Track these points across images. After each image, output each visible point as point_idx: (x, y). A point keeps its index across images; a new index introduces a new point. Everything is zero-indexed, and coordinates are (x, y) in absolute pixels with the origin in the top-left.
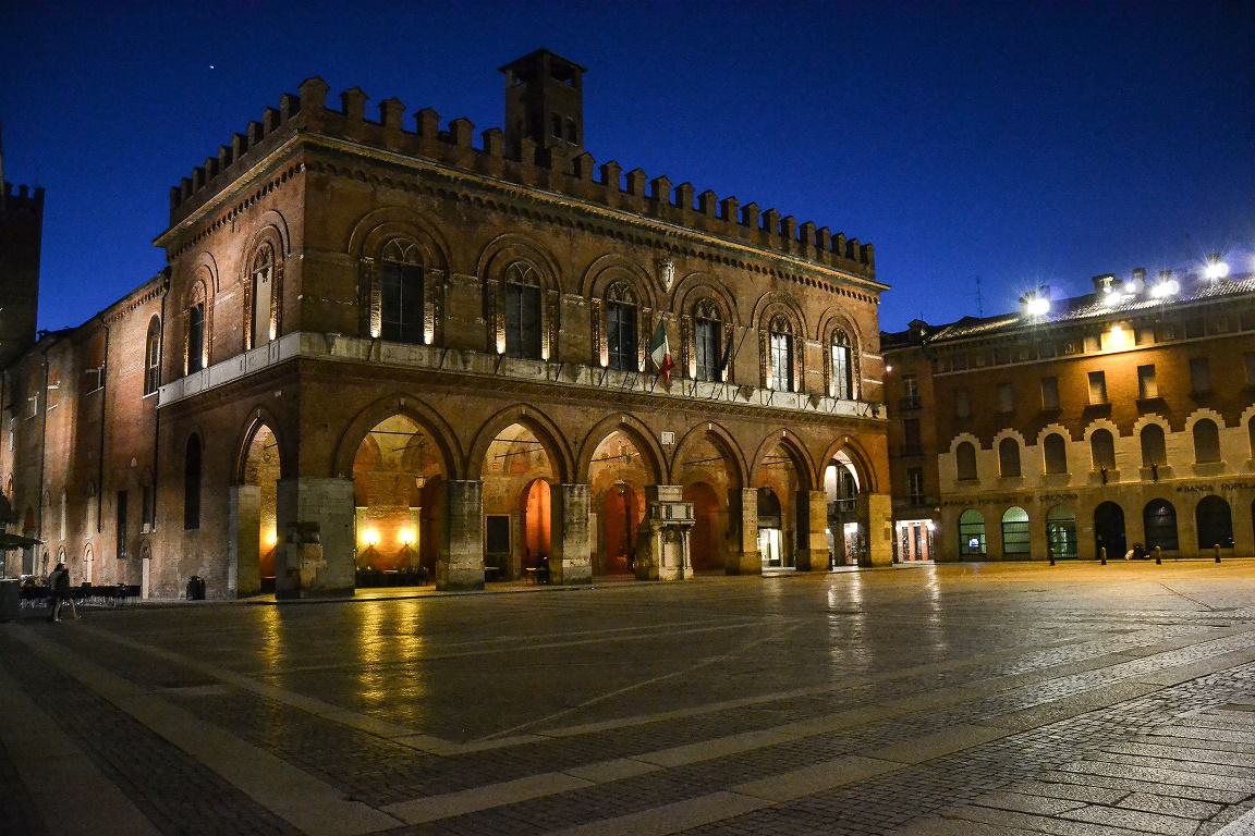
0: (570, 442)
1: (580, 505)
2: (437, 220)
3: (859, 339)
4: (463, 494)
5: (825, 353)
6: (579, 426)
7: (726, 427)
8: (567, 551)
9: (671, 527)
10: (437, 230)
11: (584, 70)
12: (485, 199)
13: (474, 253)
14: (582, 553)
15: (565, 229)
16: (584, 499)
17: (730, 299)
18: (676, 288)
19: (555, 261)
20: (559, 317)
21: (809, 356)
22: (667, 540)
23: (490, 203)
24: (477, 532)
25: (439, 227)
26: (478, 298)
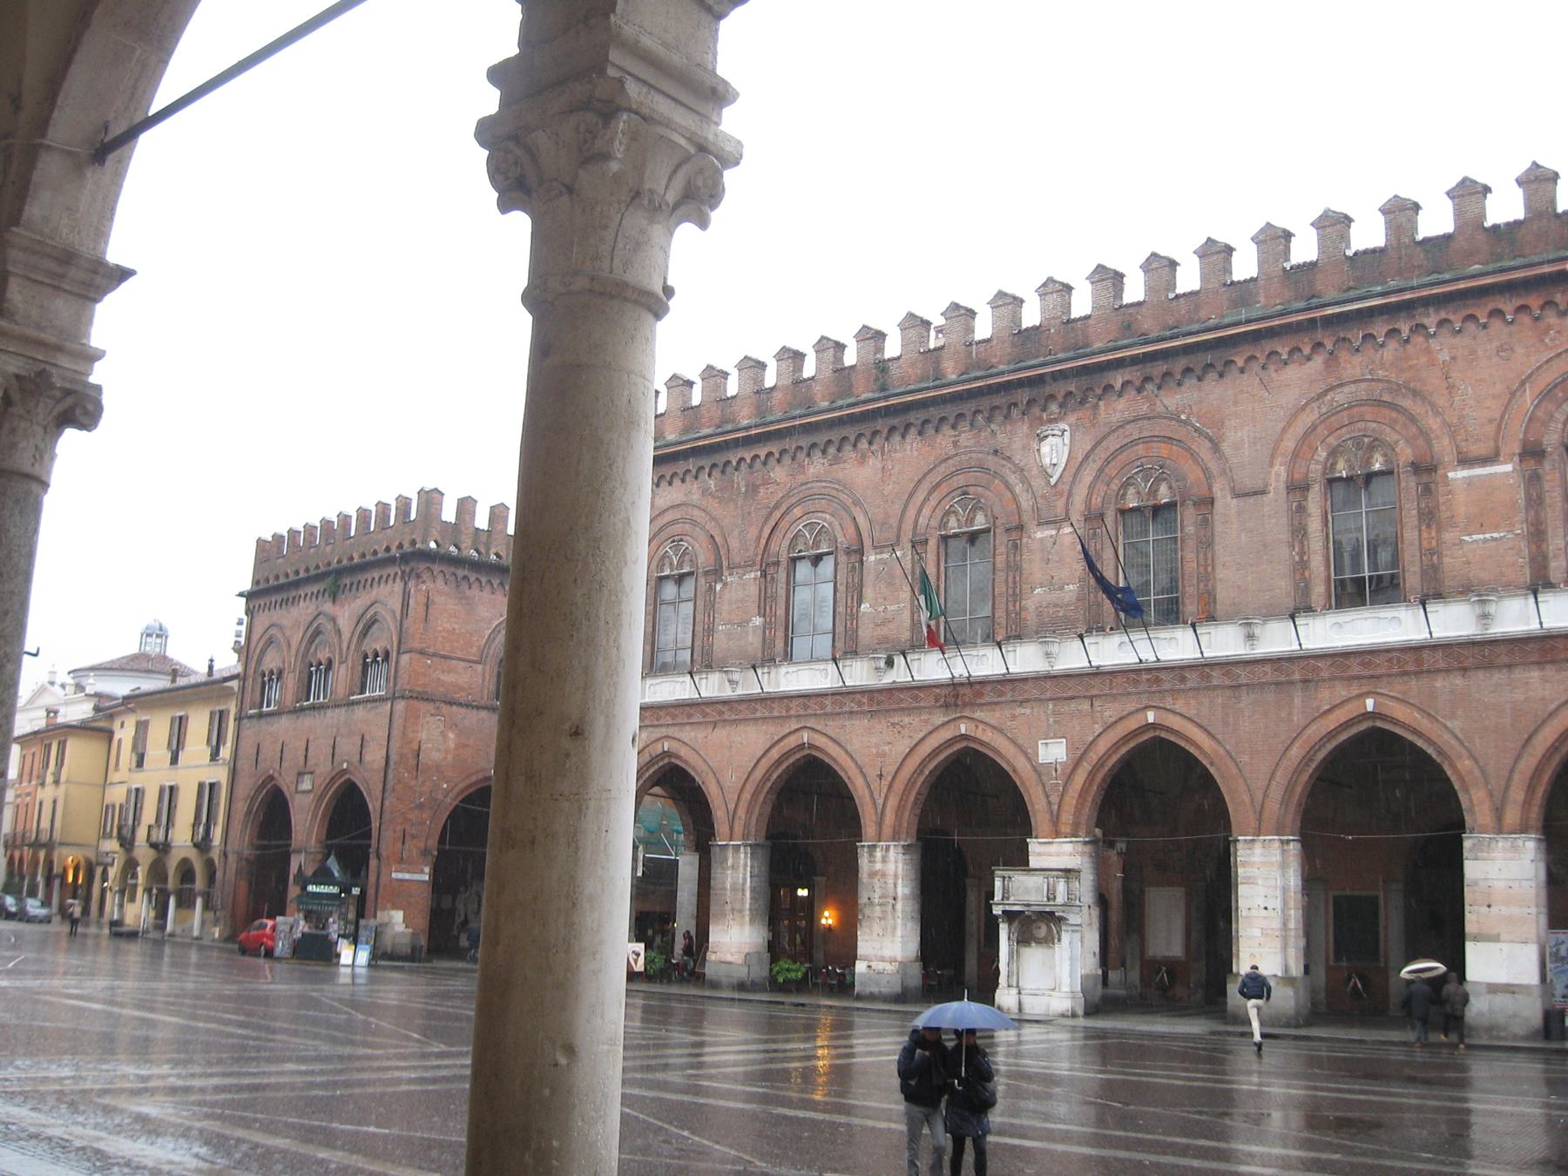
0: (872, 773)
1: (884, 875)
2: (713, 505)
4: (726, 860)
6: (886, 748)
7: (1192, 713)
8: (863, 947)
10: (713, 519)
12: (762, 453)
13: (753, 532)
14: (887, 953)
15: (874, 447)
16: (891, 867)
17: (1203, 449)
18: (1075, 467)
19: (857, 503)
21: (1461, 505)
23: (770, 454)
24: (741, 911)
25: (714, 513)
26: (753, 590)
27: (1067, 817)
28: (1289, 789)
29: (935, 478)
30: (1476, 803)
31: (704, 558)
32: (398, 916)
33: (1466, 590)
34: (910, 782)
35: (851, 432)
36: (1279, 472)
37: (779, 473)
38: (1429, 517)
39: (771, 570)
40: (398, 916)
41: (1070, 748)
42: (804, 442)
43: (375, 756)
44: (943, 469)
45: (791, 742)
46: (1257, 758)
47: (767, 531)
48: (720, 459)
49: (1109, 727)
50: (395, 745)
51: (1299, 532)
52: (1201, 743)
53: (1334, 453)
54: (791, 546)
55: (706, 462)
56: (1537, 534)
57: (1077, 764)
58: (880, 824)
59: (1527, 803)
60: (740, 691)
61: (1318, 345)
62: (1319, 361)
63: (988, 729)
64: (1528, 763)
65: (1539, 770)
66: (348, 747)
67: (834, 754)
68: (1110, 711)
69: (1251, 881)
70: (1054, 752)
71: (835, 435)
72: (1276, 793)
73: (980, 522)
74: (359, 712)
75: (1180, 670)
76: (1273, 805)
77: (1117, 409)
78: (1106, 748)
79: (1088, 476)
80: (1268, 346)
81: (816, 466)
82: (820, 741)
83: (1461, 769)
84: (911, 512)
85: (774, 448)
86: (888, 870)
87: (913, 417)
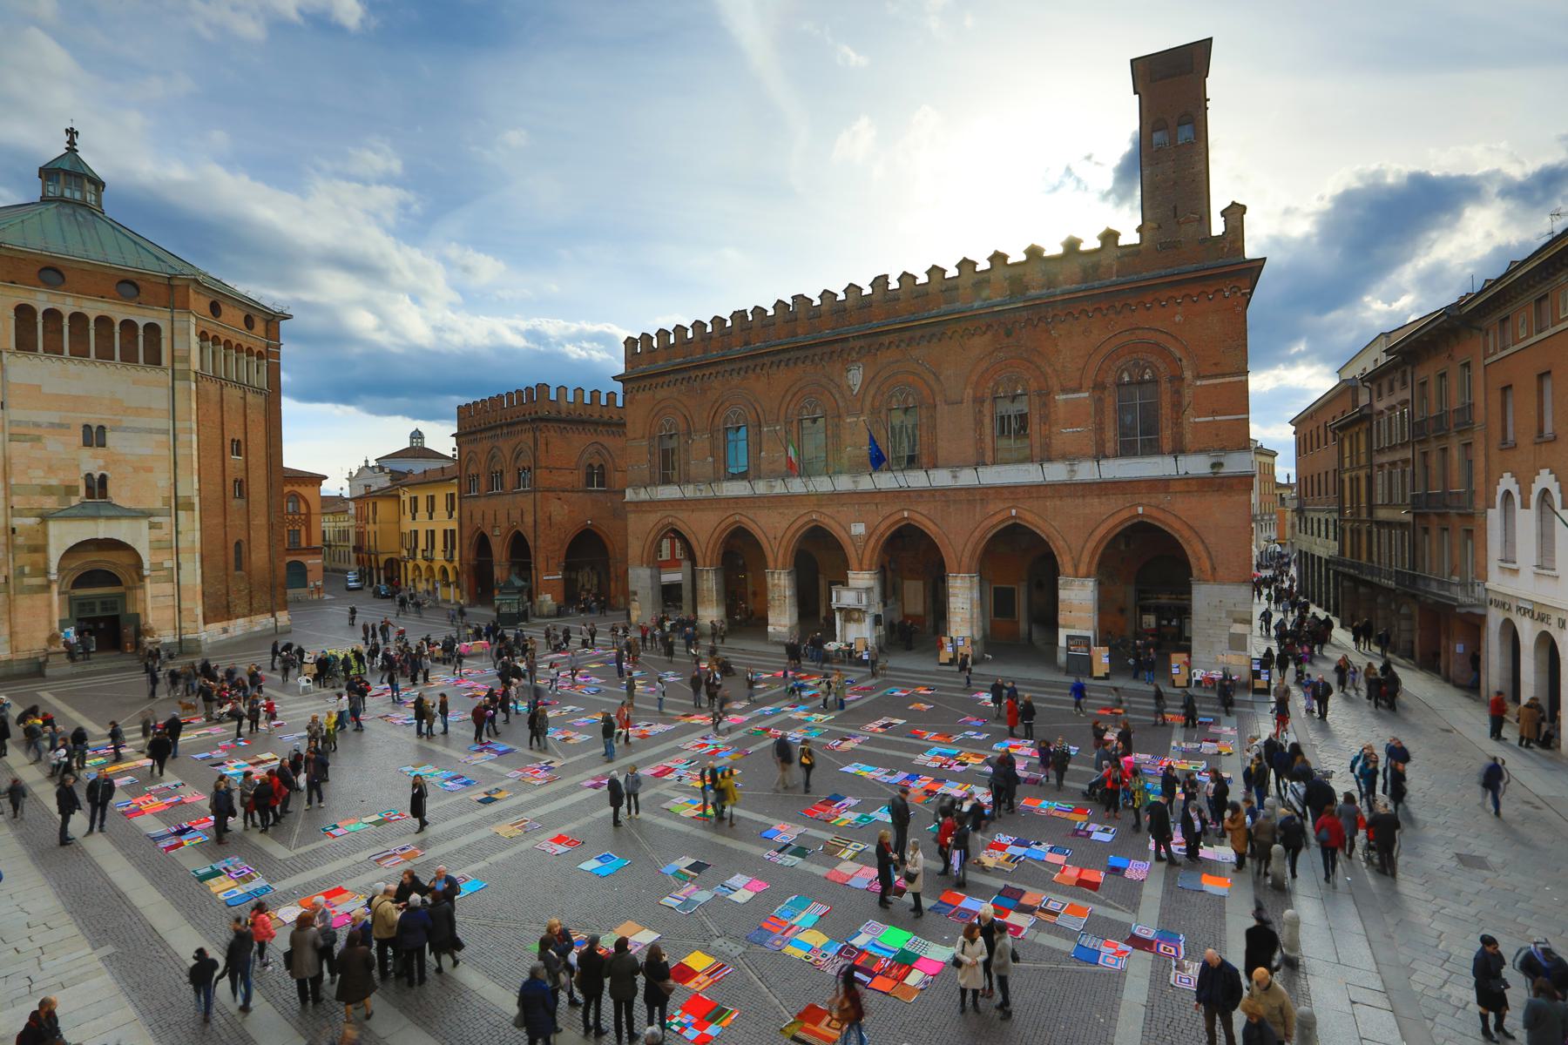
0: (771, 537)
3: (1185, 362)
5: (1099, 402)
8: (771, 620)
20: (761, 444)
27: (866, 562)
28: (974, 550)
29: (794, 389)
30: (1065, 562)
32: (548, 597)
33: (1064, 457)
34: (789, 542)
35: (751, 363)
36: (969, 391)
40: (548, 597)
42: (728, 367)
43: (529, 519)
45: (731, 520)
46: (959, 538)
48: (686, 375)
49: (887, 519)
50: (539, 514)
52: (930, 528)
53: (997, 384)
55: (679, 377)
56: (1100, 429)
57: (870, 536)
58: (776, 561)
59: (1090, 563)
61: (989, 326)
62: (988, 336)
64: (1091, 545)
65: (1096, 547)
66: (515, 514)
67: (751, 527)
68: (886, 510)
69: (955, 595)
70: (859, 529)
71: (744, 365)
72: (967, 554)
74: (519, 497)
75: (920, 493)
76: (966, 560)
78: (885, 528)
79: (872, 391)
82: (744, 519)
83: (1058, 546)
84: (784, 405)
85: (713, 370)
86: (781, 584)
87: (781, 357)
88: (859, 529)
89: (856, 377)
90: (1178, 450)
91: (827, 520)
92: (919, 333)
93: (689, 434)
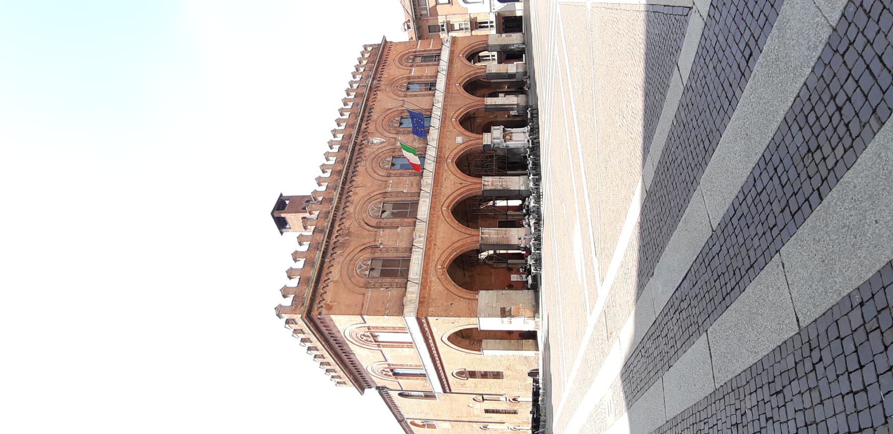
0: (460, 186)
2: (348, 250)
9: (504, 137)
11: (281, 195)
19: (369, 194)
21: (419, 74)
22: (511, 139)
26: (387, 231)
27: (478, 136)
31: (367, 255)
35: (344, 197)
37: (347, 223)
38: (419, 77)
39: (382, 225)
41: (459, 136)
44: (370, 170)
45: (445, 213)
47: (367, 227)
51: (416, 96)
52: (462, 112)
54: (376, 217)
55: (330, 251)
58: (476, 183)
60: (423, 234)
63: (451, 155)
70: (459, 140)
71: (343, 201)
73: (390, 159)
75: (444, 113)
77: (371, 128)
78: (462, 129)
80: (371, 99)
81: (351, 209)
82: (446, 204)
88: (459, 140)
89: (376, 140)
90: (440, 50)
91: (453, 154)
92: (367, 114)
93: (376, 247)
